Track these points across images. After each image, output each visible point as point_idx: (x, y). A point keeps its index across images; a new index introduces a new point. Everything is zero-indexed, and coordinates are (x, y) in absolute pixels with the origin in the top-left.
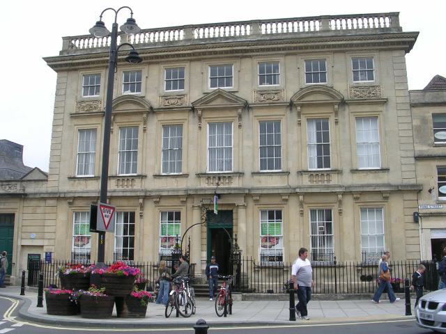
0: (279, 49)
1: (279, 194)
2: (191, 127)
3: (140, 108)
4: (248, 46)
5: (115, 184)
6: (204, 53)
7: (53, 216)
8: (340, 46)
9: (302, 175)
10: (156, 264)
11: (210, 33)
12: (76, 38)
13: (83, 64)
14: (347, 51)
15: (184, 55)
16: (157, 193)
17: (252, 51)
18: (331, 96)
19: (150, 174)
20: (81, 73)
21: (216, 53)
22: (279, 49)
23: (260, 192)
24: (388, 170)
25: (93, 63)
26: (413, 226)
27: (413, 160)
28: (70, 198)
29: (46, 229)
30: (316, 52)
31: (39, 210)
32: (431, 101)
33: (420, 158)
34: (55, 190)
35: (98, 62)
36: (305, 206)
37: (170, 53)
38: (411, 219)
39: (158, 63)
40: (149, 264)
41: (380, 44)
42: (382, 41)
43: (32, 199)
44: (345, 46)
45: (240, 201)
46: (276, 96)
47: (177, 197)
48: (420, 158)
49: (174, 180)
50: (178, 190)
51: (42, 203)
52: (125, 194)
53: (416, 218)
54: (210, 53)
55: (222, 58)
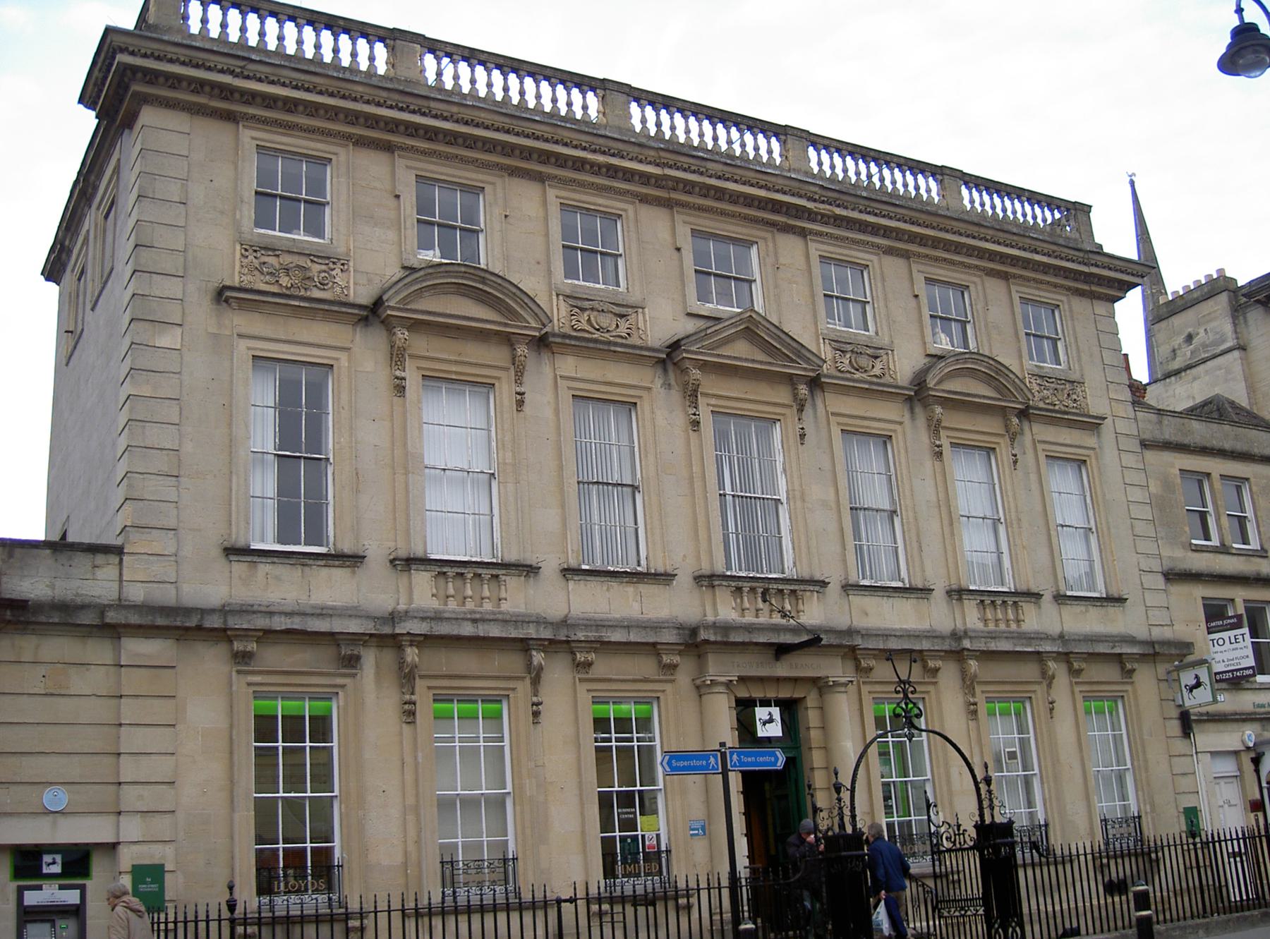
0: (875, 230)
1: (332, 634)
2: (661, 417)
3: (761, 357)
4: (810, 199)
5: (993, 624)
6: (688, 187)
7: (160, 711)
8: (1003, 258)
9: (960, 599)
10: (593, 891)
11: (460, 77)
12: (433, 46)
13: (270, 102)
14: (1015, 276)
15: (629, 175)
16: (592, 635)
17: (811, 216)
18: (1001, 389)
19: (550, 564)
20: (249, 137)
21: (720, 194)
22: (875, 230)
23: (261, 622)
24: (1120, 600)
25: (313, 110)
26: (1180, 745)
27: (1160, 582)
28: (245, 634)
29: (128, 769)
30: (953, 263)
31: (79, 682)
32: (1173, 439)
33: (1175, 576)
34: (166, 596)
35: (333, 113)
36: (420, 684)
37: (590, 156)
38: (1175, 727)
39: (540, 178)
40: (396, 904)
41: (1077, 275)
42: (1085, 269)
43: (45, 629)
44: (1014, 261)
45: (835, 669)
46: (622, 322)
47: (653, 649)
48: (1175, 576)
49: (630, 589)
50: (656, 626)
51: (99, 651)
52: (482, 630)
53: (1187, 723)
54: (706, 191)
55: (733, 215)
